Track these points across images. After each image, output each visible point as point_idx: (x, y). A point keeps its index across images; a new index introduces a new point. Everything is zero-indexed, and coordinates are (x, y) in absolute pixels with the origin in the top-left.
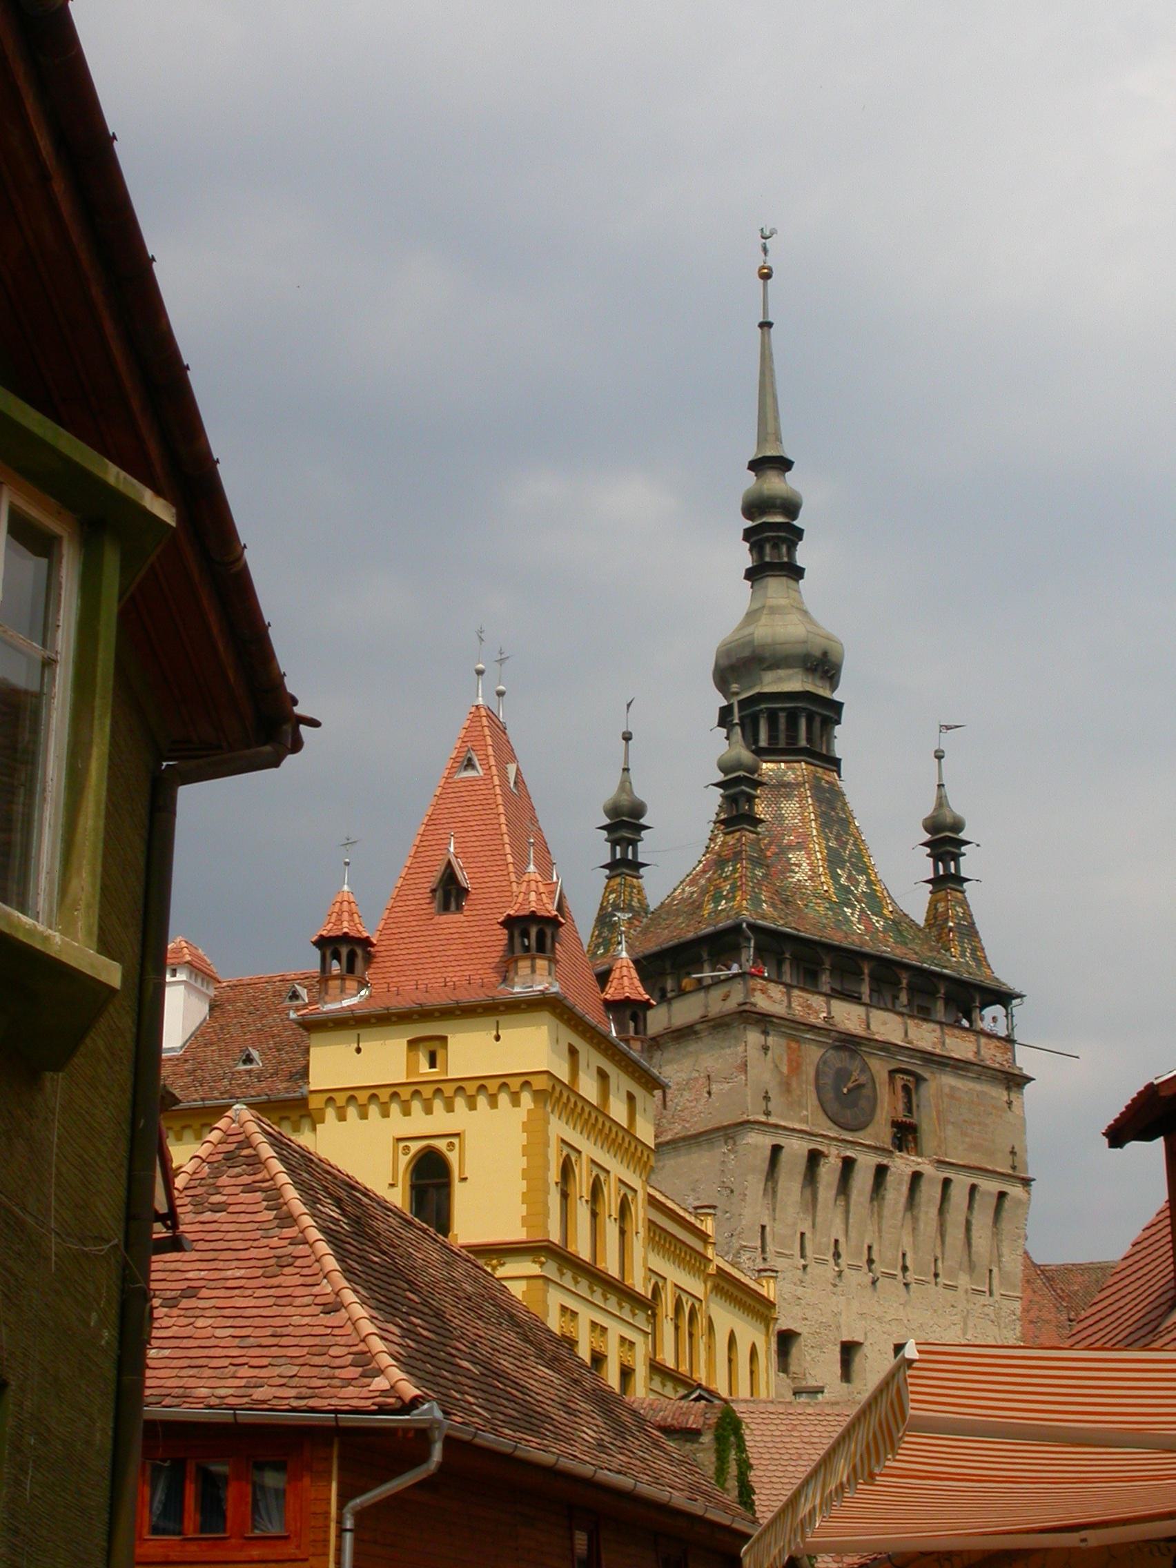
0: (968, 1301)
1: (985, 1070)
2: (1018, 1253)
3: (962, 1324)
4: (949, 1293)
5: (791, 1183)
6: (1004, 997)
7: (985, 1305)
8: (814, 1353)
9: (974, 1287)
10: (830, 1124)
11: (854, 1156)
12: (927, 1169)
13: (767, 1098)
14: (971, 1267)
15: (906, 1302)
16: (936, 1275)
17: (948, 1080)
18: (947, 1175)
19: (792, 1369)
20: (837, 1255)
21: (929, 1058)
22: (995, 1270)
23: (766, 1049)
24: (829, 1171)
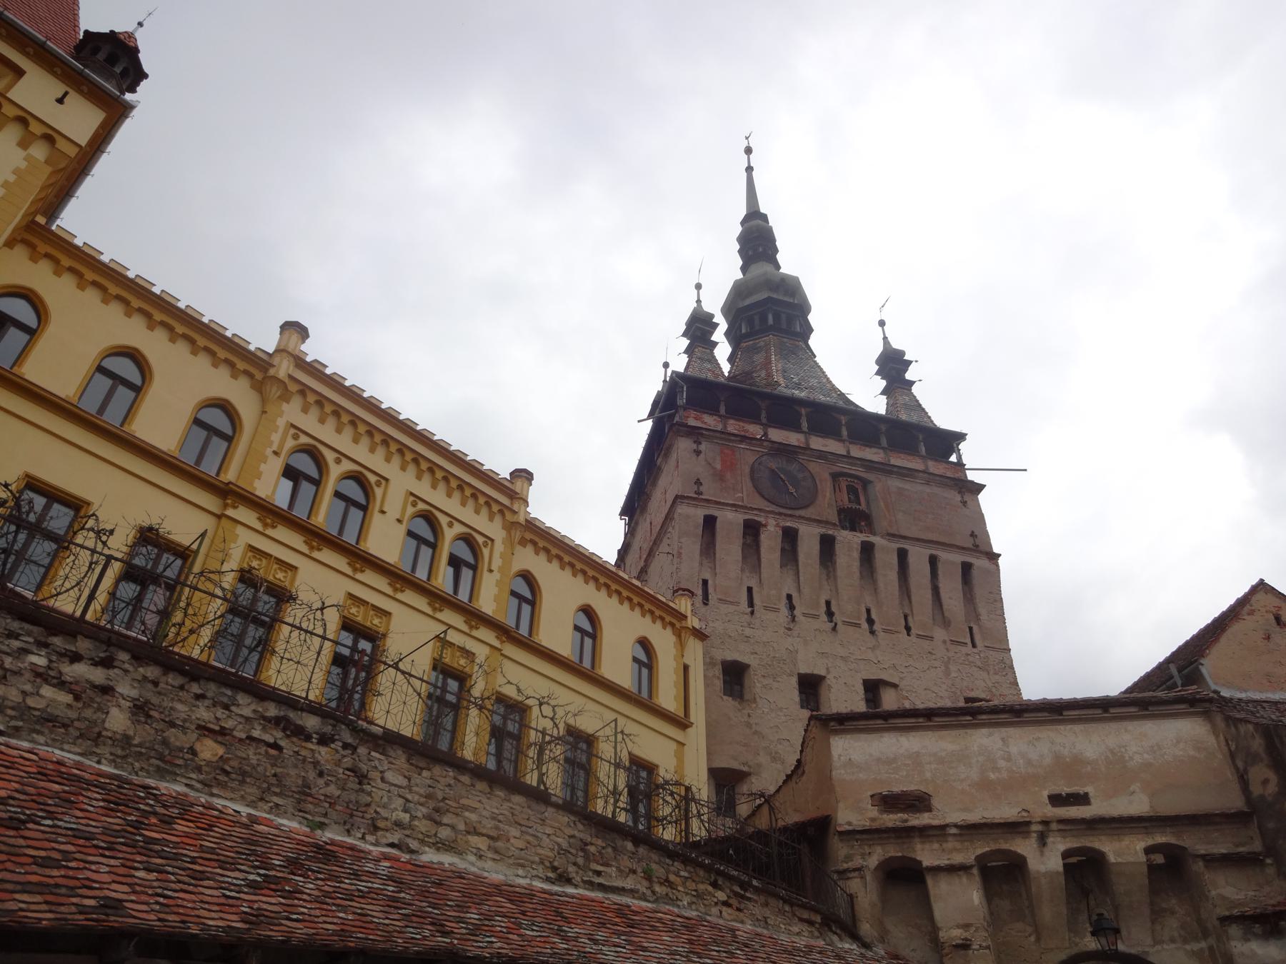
0: (947, 650)
1: (931, 477)
2: (997, 613)
3: (943, 668)
4: (926, 644)
5: (730, 548)
6: (951, 440)
7: (968, 655)
8: (766, 682)
9: (953, 639)
10: (766, 503)
11: (794, 526)
12: (876, 540)
13: (698, 483)
14: (946, 623)
15: (874, 646)
16: (908, 629)
17: (894, 483)
18: (902, 546)
19: (747, 696)
20: (792, 607)
21: (869, 465)
22: (975, 629)
23: (698, 453)
24: (770, 541)
